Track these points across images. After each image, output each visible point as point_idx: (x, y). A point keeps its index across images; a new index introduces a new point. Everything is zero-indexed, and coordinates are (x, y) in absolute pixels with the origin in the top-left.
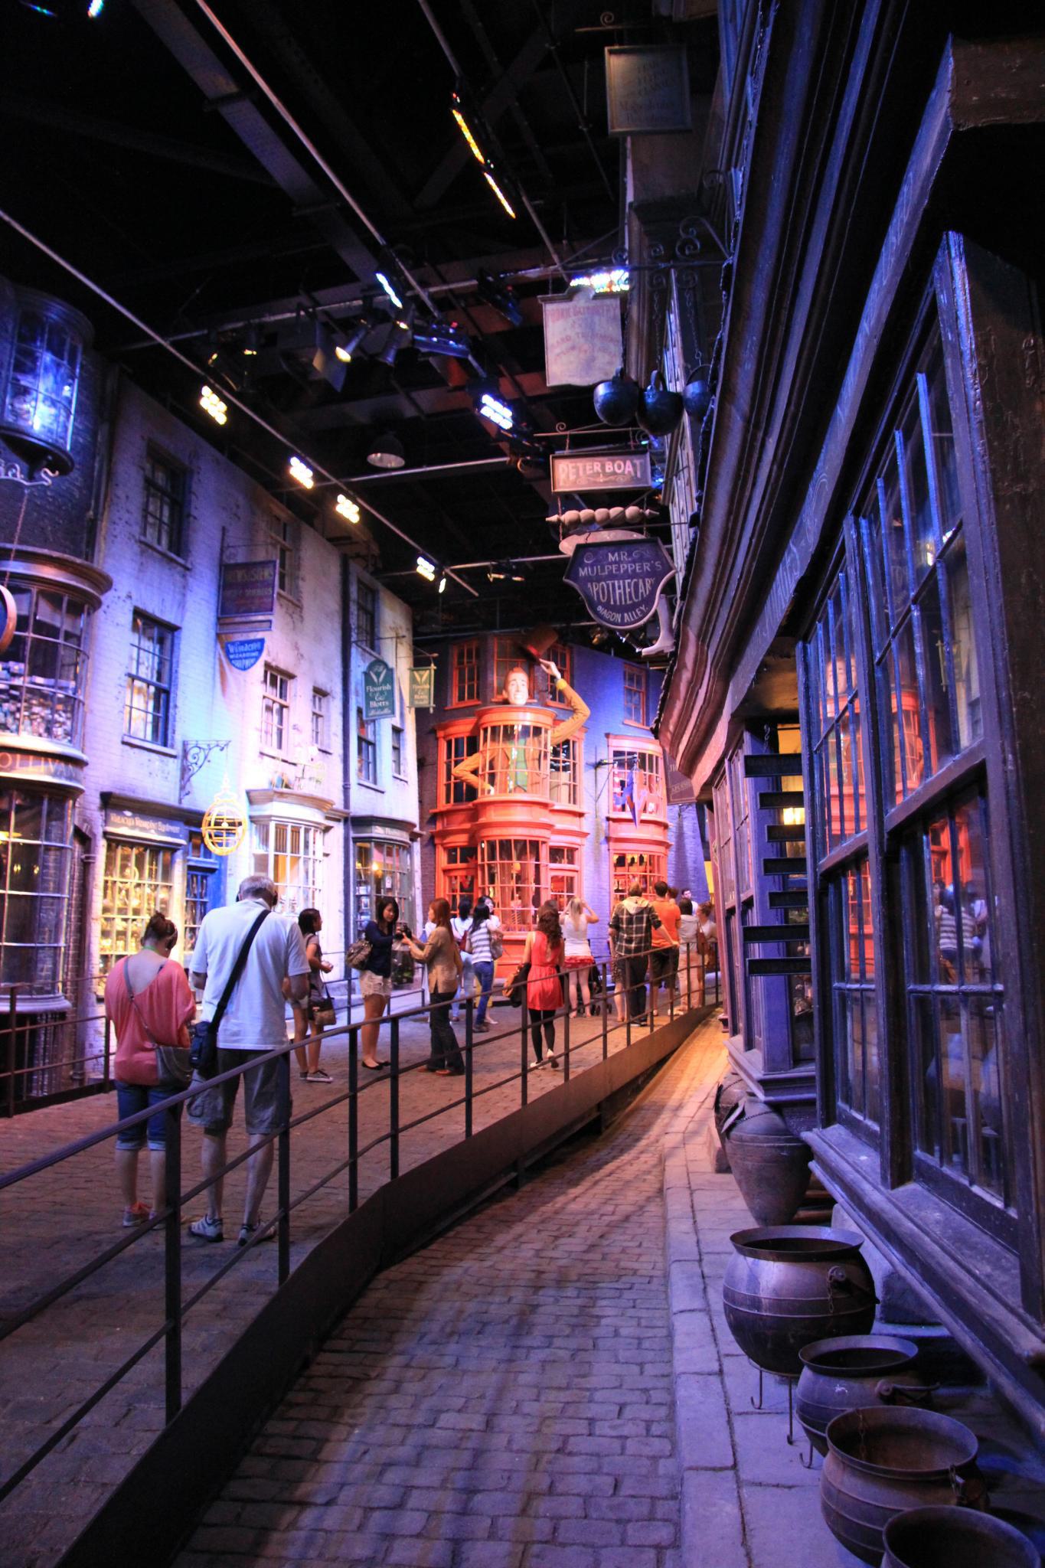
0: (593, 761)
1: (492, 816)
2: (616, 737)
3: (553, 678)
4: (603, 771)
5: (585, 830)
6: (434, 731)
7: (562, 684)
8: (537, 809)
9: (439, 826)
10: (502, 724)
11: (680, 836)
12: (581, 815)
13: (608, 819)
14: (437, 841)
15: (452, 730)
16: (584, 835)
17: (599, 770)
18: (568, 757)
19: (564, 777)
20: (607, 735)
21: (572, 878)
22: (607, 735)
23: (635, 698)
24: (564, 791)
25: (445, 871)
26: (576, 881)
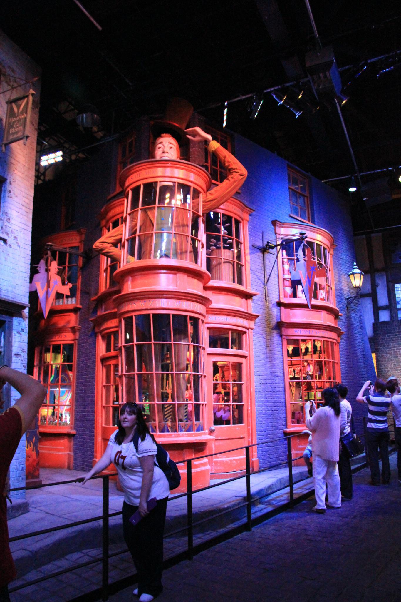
0: (260, 244)
1: (130, 287)
2: (284, 225)
3: (206, 142)
4: (270, 258)
5: (252, 311)
6: (99, 223)
7: (215, 145)
8: (182, 278)
9: (99, 313)
10: (141, 183)
11: (349, 326)
12: (248, 296)
13: (279, 304)
14: (97, 330)
15: (111, 214)
16: (251, 317)
17: (267, 255)
18: (230, 233)
19: (226, 254)
20: (274, 223)
21: (240, 364)
22: (274, 223)
23: (301, 201)
24: (226, 271)
25: (104, 360)
26: (244, 366)
